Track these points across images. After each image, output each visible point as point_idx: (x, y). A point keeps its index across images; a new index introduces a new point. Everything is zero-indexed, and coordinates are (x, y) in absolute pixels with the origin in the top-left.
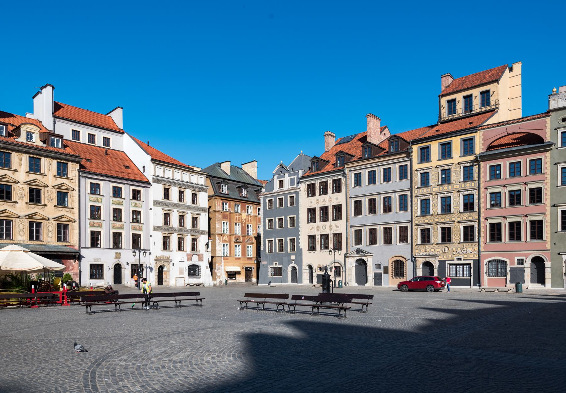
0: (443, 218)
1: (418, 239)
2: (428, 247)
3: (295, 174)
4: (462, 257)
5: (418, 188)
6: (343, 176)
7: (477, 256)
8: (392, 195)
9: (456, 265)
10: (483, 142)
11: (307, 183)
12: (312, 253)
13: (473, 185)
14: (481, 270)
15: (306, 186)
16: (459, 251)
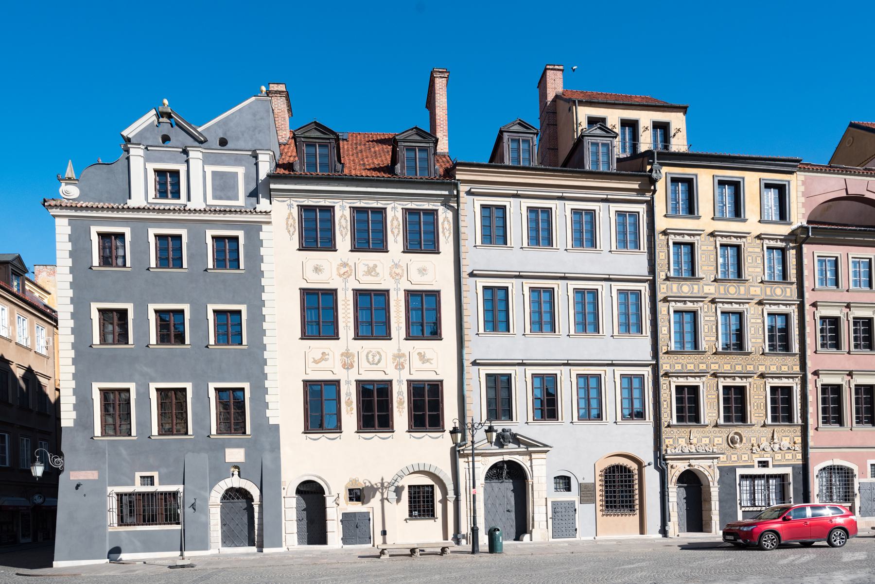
0: (727, 364)
1: (670, 413)
2: (696, 433)
3: (237, 161)
4: (770, 460)
5: (667, 279)
6: (446, 204)
7: (800, 456)
8: (603, 288)
9: (753, 478)
10: (803, 200)
11: (295, 202)
12: (323, 440)
13: (788, 294)
14: (811, 489)
15: (295, 212)
16: (765, 444)
